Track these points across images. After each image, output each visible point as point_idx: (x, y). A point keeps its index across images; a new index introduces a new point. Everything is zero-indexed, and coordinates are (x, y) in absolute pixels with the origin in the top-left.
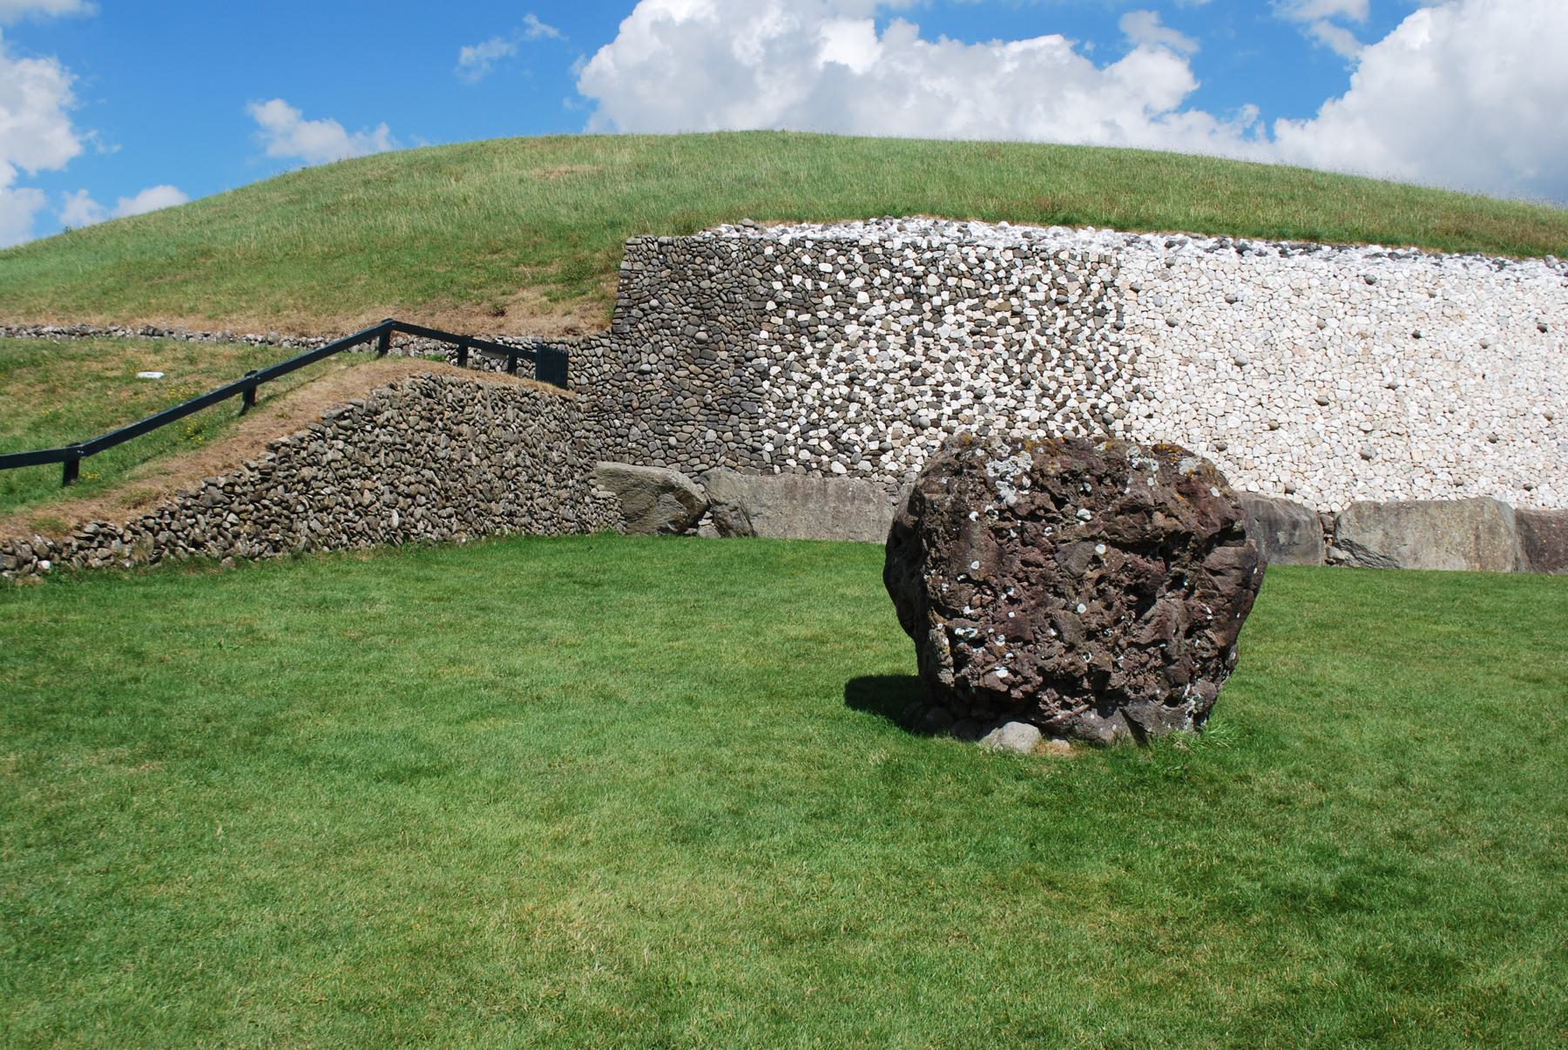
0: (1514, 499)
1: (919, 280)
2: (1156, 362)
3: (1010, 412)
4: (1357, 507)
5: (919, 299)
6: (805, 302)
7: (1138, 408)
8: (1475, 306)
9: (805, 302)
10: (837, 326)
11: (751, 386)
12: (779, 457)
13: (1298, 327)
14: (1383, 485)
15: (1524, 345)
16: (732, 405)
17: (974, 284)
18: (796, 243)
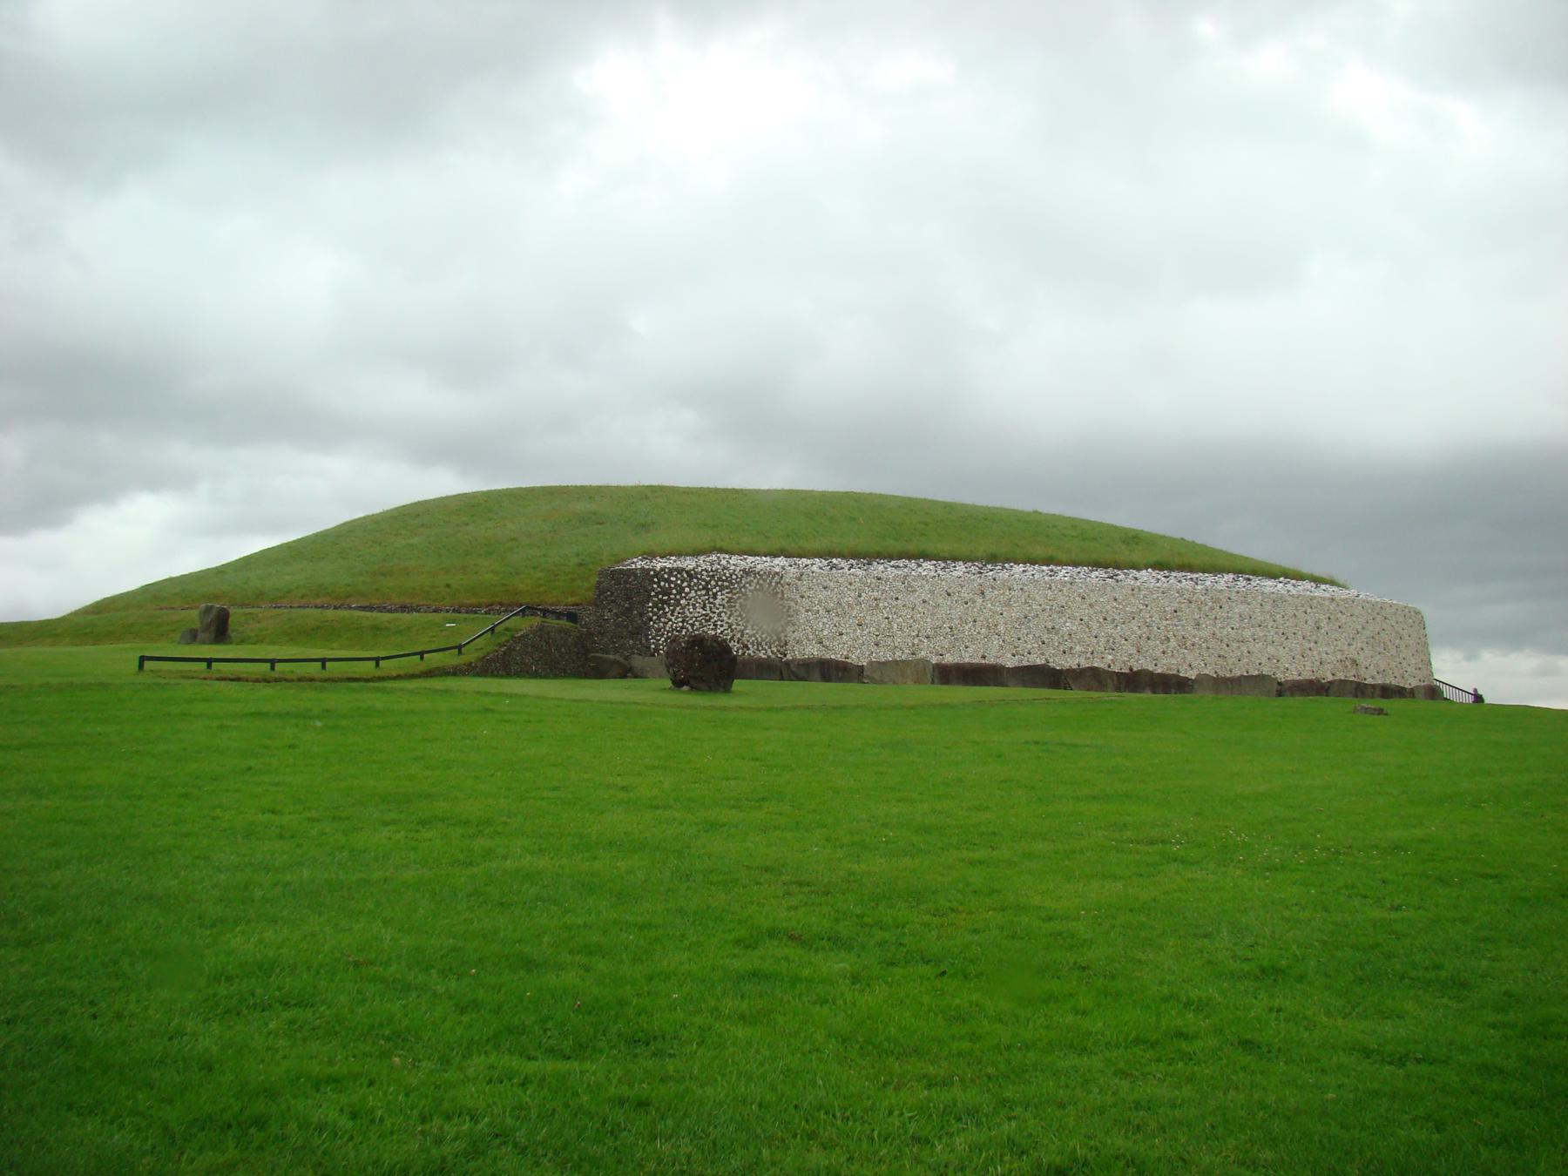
0: (934, 660)
1: (708, 583)
2: (796, 611)
3: (742, 632)
4: (871, 663)
5: (708, 590)
6: (667, 592)
7: (790, 629)
8: (922, 587)
9: (667, 592)
10: (678, 603)
11: (646, 623)
12: (657, 650)
13: (850, 597)
14: (884, 655)
15: (941, 601)
16: (640, 631)
17: (727, 582)
18: (663, 569)
